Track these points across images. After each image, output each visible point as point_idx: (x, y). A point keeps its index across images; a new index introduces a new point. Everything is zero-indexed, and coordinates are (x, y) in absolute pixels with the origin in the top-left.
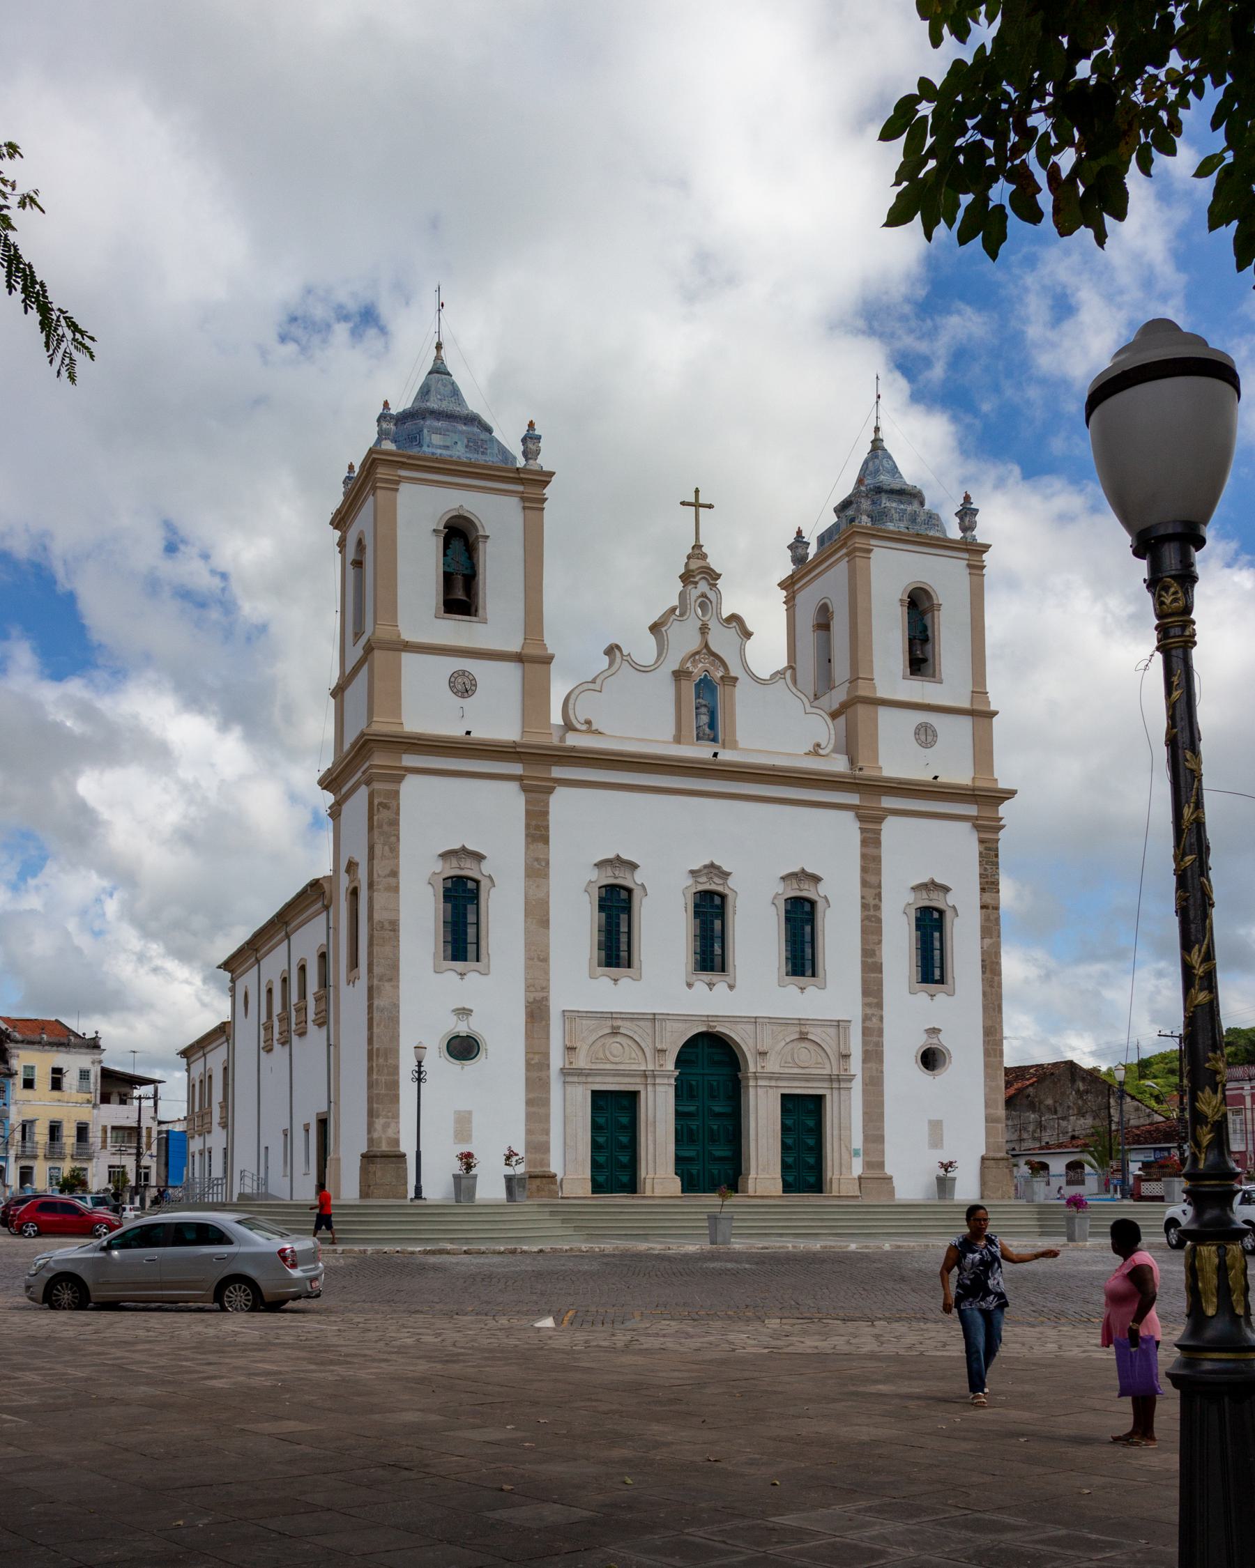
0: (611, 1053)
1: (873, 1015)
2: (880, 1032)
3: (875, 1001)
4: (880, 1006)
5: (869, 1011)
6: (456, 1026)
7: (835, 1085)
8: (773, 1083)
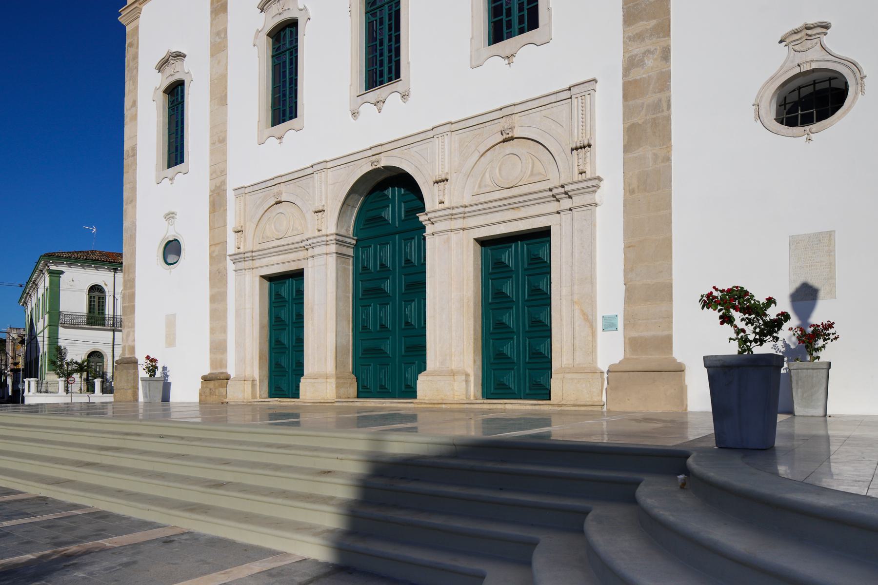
0: (275, 227)
1: (648, 52)
2: (664, 81)
3: (653, 22)
4: (664, 29)
5: (637, 49)
6: (167, 234)
7: (566, 203)
8: (459, 223)
